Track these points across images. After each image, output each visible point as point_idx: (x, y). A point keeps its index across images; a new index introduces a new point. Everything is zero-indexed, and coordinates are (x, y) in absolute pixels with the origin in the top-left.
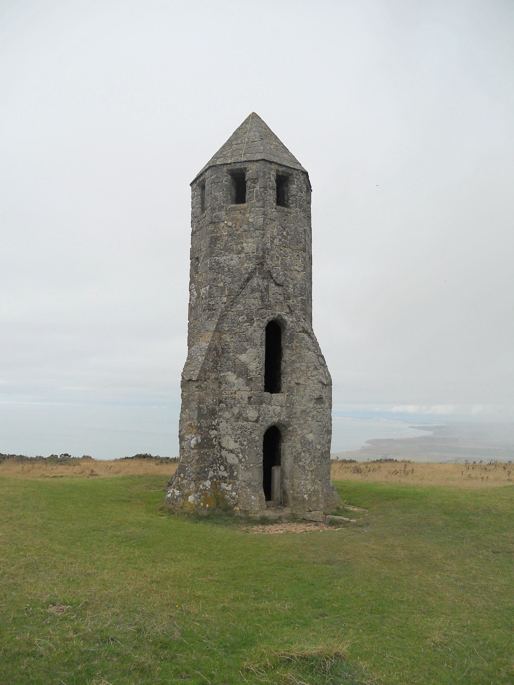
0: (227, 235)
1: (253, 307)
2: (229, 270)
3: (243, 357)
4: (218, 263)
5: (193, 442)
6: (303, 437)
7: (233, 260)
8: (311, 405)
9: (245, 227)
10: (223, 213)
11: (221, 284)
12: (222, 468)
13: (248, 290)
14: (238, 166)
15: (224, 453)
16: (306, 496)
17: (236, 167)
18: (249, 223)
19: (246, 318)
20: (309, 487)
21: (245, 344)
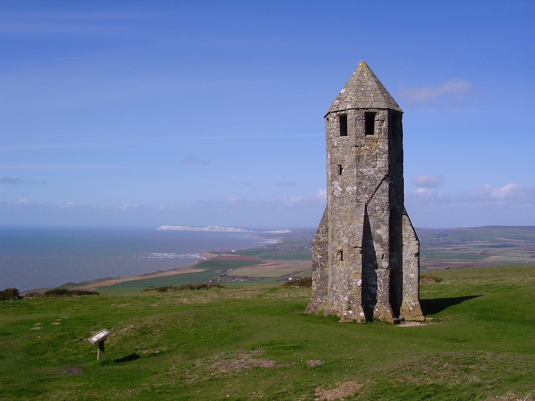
0: (366, 155)
1: (384, 201)
2: (369, 178)
3: (379, 231)
4: (361, 173)
5: (360, 282)
6: (407, 275)
7: (368, 171)
8: (413, 258)
9: (377, 151)
10: (363, 140)
11: (364, 187)
12: (368, 296)
13: (379, 190)
14: (372, 110)
15: (369, 287)
16: (411, 308)
17: (370, 111)
18: (379, 149)
19: (380, 208)
20: (412, 303)
21: (380, 223)
